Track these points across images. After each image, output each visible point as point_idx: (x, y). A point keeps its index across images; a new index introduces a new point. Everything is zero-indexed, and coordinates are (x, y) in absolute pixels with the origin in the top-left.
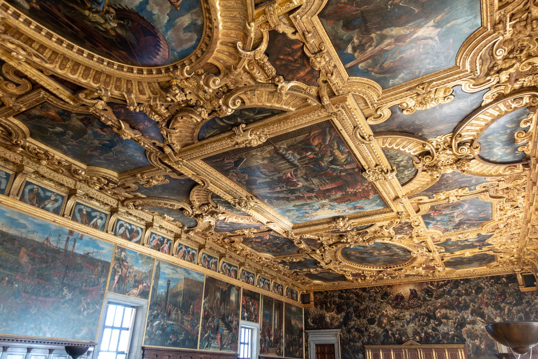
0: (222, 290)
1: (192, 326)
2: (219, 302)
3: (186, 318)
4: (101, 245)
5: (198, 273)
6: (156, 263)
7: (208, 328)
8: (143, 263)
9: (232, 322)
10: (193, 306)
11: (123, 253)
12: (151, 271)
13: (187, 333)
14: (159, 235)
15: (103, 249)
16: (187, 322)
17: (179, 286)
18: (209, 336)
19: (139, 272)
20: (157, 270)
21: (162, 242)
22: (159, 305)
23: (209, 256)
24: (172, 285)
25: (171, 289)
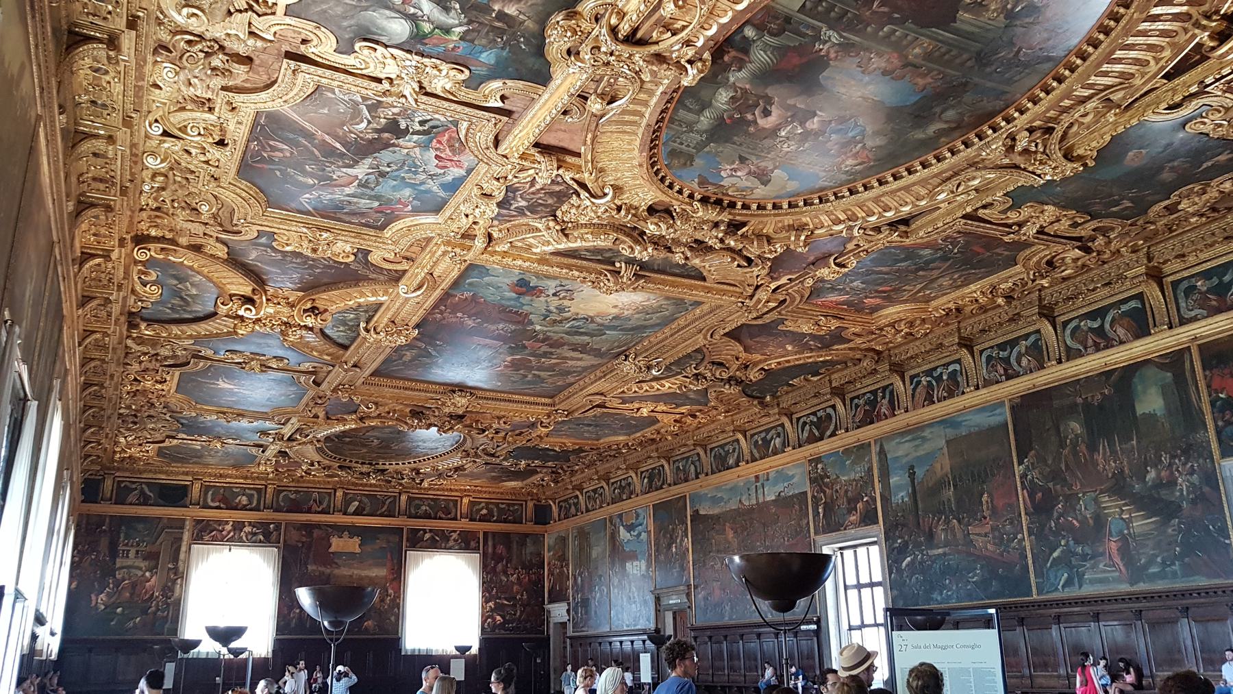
0: (1087, 405)
1: (999, 541)
2: (1083, 447)
3: (977, 530)
4: (791, 473)
5: (983, 410)
6: (874, 449)
7: (1057, 533)
8: (853, 463)
9: (1172, 483)
10: (990, 495)
11: (820, 466)
12: (870, 469)
13: (991, 564)
14: (864, 394)
15: (793, 476)
16: (980, 539)
17: (938, 466)
18: (1069, 553)
19: (849, 482)
20: (880, 460)
21: (873, 403)
22: (903, 525)
23: (1002, 347)
24: (920, 473)
25: (922, 482)
